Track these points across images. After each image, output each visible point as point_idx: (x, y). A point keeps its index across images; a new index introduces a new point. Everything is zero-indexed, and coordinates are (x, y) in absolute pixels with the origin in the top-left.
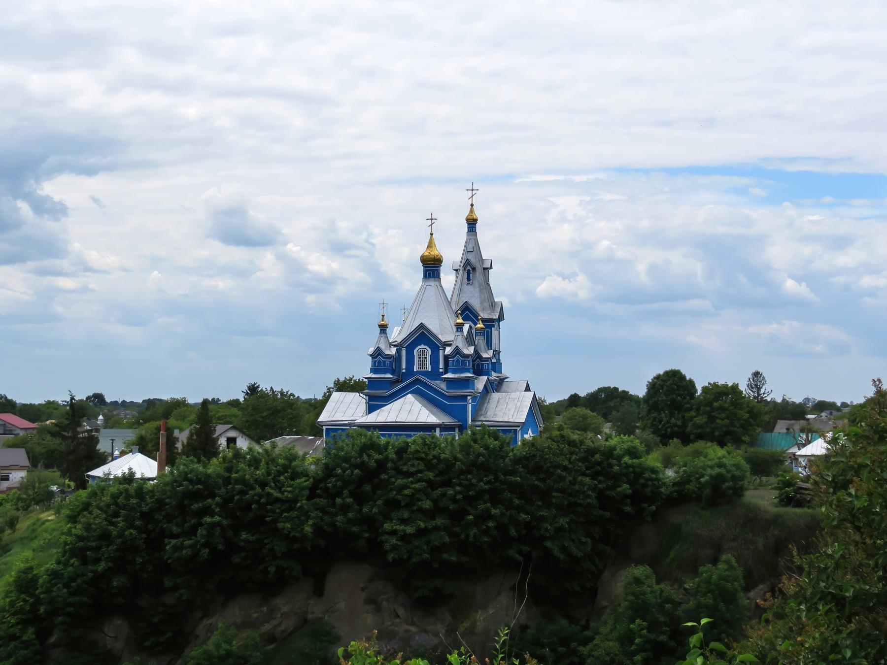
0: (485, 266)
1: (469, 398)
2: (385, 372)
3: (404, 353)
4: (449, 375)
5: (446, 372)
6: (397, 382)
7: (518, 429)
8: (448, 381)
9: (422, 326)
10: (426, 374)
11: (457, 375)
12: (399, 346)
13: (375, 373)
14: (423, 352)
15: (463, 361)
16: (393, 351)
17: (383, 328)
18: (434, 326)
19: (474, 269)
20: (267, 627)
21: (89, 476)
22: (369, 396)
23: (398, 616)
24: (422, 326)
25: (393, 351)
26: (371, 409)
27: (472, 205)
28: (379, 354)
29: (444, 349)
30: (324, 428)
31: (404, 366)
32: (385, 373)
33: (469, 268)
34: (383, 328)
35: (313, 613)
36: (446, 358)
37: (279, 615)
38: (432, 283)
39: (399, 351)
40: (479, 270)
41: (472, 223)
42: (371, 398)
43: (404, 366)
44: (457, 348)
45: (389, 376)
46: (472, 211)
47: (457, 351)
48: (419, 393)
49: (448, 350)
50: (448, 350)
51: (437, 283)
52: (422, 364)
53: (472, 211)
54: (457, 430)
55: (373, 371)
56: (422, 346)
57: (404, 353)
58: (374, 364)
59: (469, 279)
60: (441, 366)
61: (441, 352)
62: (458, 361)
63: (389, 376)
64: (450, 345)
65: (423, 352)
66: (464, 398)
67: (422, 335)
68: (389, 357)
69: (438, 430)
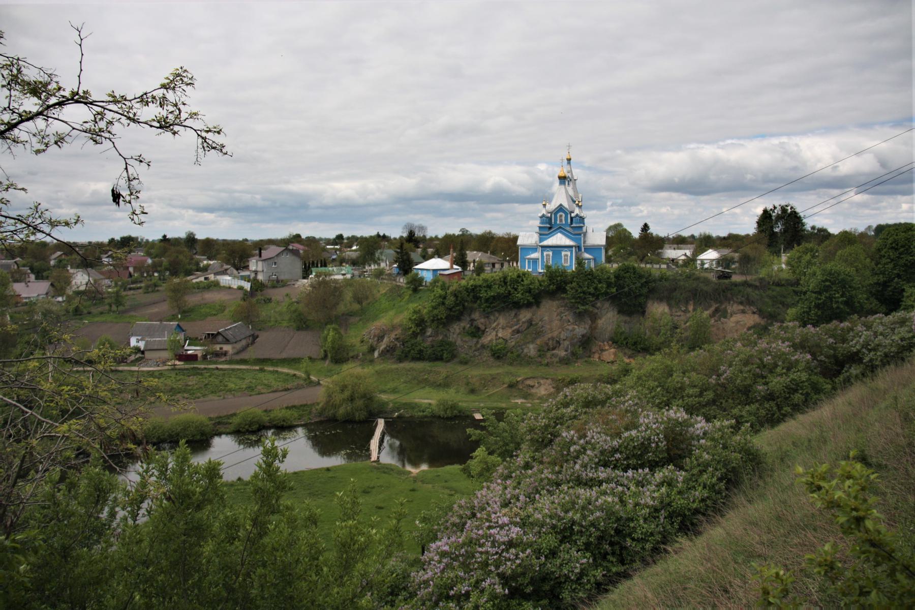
4: (574, 225)
6: (550, 228)
9: (561, 205)
12: (551, 213)
18: (566, 205)
20: (515, 327)
24: (561, 205)
36: (572, 218)
41: (569, 160)
42: (541, 234)
45: (549, 225)
48: (561, 232)
49: (573, 215)
50: (573, 215)
52: (561, 220)
55: (542, 223)
67: (561, 208)
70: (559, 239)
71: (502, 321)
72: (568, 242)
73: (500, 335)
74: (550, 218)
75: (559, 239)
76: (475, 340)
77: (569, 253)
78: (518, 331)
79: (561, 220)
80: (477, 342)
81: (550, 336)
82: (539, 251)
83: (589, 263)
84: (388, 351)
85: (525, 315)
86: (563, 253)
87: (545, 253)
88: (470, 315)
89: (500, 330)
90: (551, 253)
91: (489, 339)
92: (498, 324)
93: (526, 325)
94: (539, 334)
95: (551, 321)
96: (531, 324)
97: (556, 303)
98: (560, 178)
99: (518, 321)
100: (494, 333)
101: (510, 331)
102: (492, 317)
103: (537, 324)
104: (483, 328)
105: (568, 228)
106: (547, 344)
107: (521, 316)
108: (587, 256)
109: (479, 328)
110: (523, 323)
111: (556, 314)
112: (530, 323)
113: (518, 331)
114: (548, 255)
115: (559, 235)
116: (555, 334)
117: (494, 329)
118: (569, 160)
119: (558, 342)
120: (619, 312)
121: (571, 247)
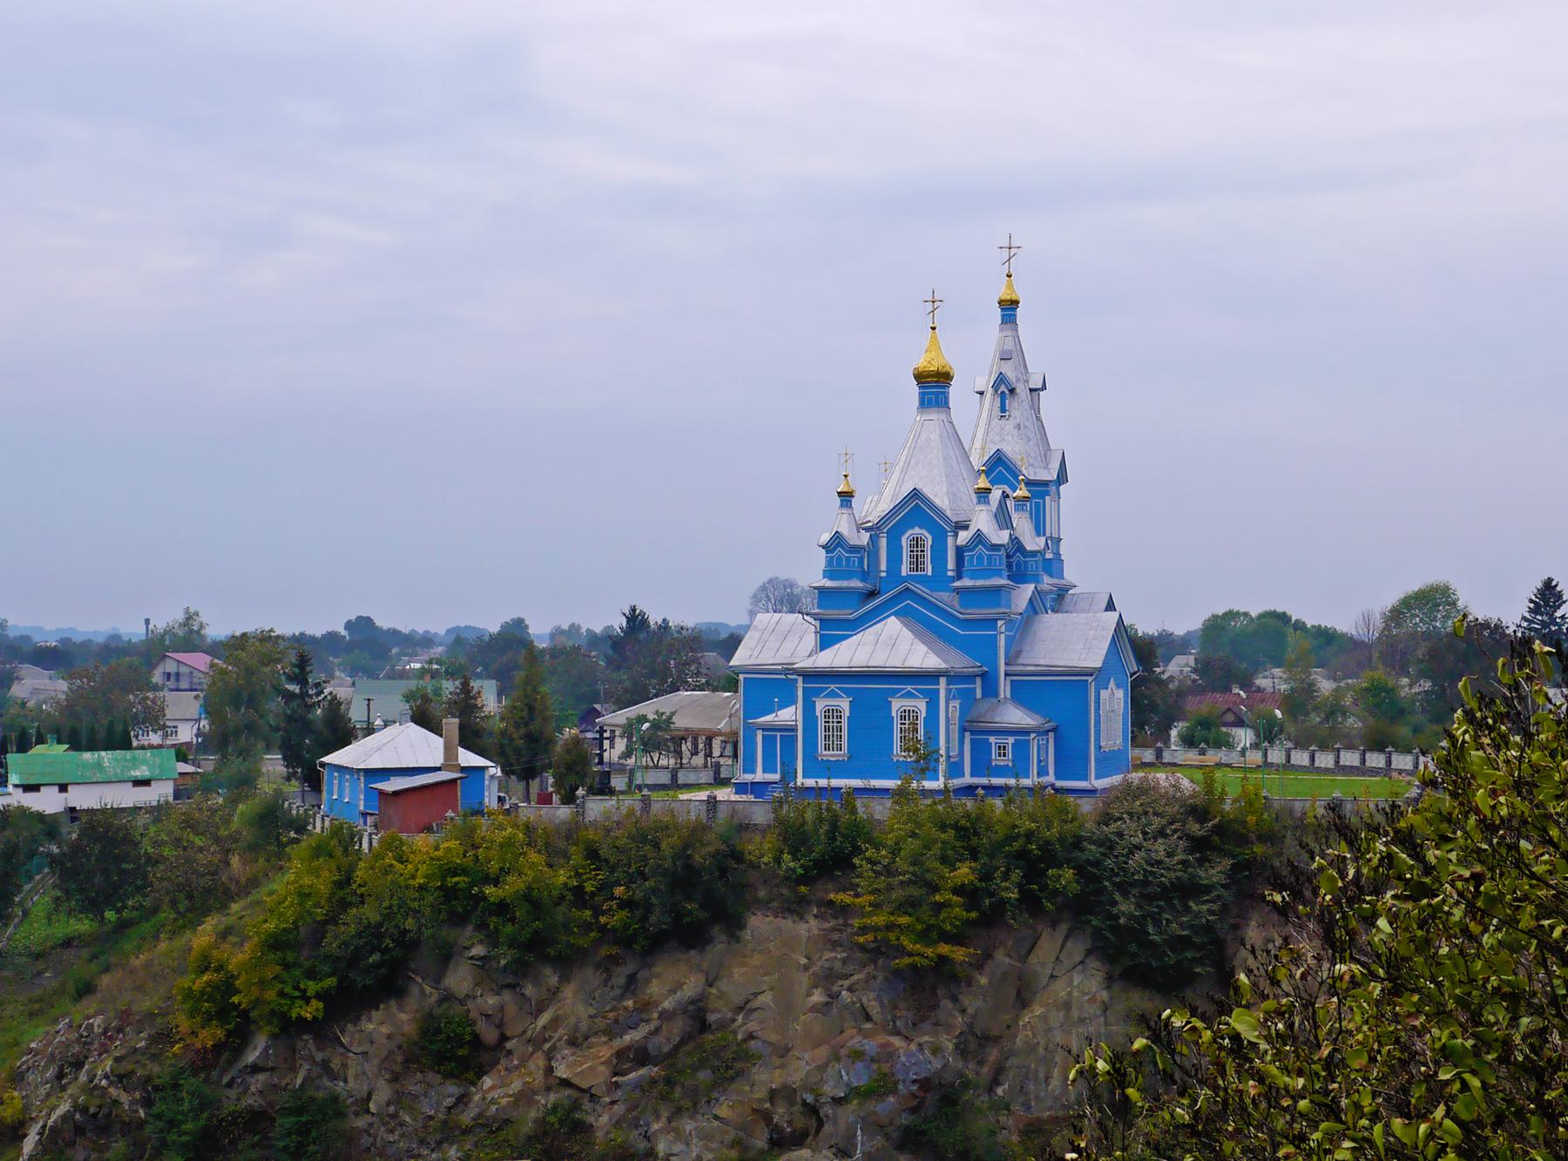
1: (1000, 623)
2: (848, 575)
3: (883, 542)
4: (966, 582)
5: (959, 577)
6: (872, 594)
7: (1090, 679)
8: (958, 590)
9: (915, 494)
10: (924, 580)
11: (980, 583)
13: (831, 579)
14: (917, 542)
15: (990, 557)
16: (864, 538)
17: (846, 497)
18: (939, 496)
19: (1012, 391)
21: (323, 765)
23: (868, 1018)
24: (915, 494)
25: (864, 538)
26: (825, 643)
27: (1009, 276)
28: (839, 544)
29: (956, 535)
30: (741, 677)
31: (883, 567)
32: (848, 579)
33: (1003, 388)
34: (846, 497)
35: (718, 1011)
36: (960, 551)
37: (656, 1015)
38: (934, 416)
39: (874, 540)
40: (1022, 391)
41: (1009, 307)
42: (825, 623)
43: (883, 567)
44: (979, 534)
45: (858, 584)
46: (1010, 286)
47: (979, 537)
49: (964, 537)
50: (964, 537)
51: (943, 416)
52: (917, 563)
53: (1010, 286)
54: (978, 681)
55: (830, 573)
56: (917, 530)
57: (883, 542)
58: (829, 562)
59: (1003, 409)
60: (951, 564)
61: (950, 540)
62: (980, 557)
63: (856, 583)
64: (966, 528)
65: (917, 542)
66: (991, 622)
67: (915, 508)
68: (856, 549)
69: (943, 681)
70: (890, 644)
71: (574, 1002)
72: (919, 655)
73: (562, 1071)
75: (890, 644)
76: (453, 1089)
77: (921, 706)
78: (641, 1056)
80: (463, 1100)
81: (776, 1079)
82: (811, 687)
83: (1022, 750)
84: (79, 1130)
85: (672, 983)
86: (897, 705)
87: (820, 705)
88: (438, 980)
89: (566, 1044)
90: (844, 705)
91: (516, 1086)
92: (555, 1022)
93: (677, 1028)
94: (731, 1065)
95: (787, 1009)
96: (704, 1027)
97: (809, 927)
98: (921, 377)
99: (645, 1007)
100: (538, 1062)
101: (606, 1052)
102: (529, 990)
103: (724, 1025)
104: (489, 1035)
105: (944, 598)
106: (767, 1117)
107: (655, 989)
108: (1016, 716)
109: (476, 1040)
110: (666, 1016)
111: (805, 980)
112: (697, 1016)
113: (641, 1056)
114: (828, 713)
115: (892, 625)
116: (799, 1070)
117: (537, 1042)
118: (1009, 307)
119: (812, 1110)
120: (1109, 980)
121: (930, 677)
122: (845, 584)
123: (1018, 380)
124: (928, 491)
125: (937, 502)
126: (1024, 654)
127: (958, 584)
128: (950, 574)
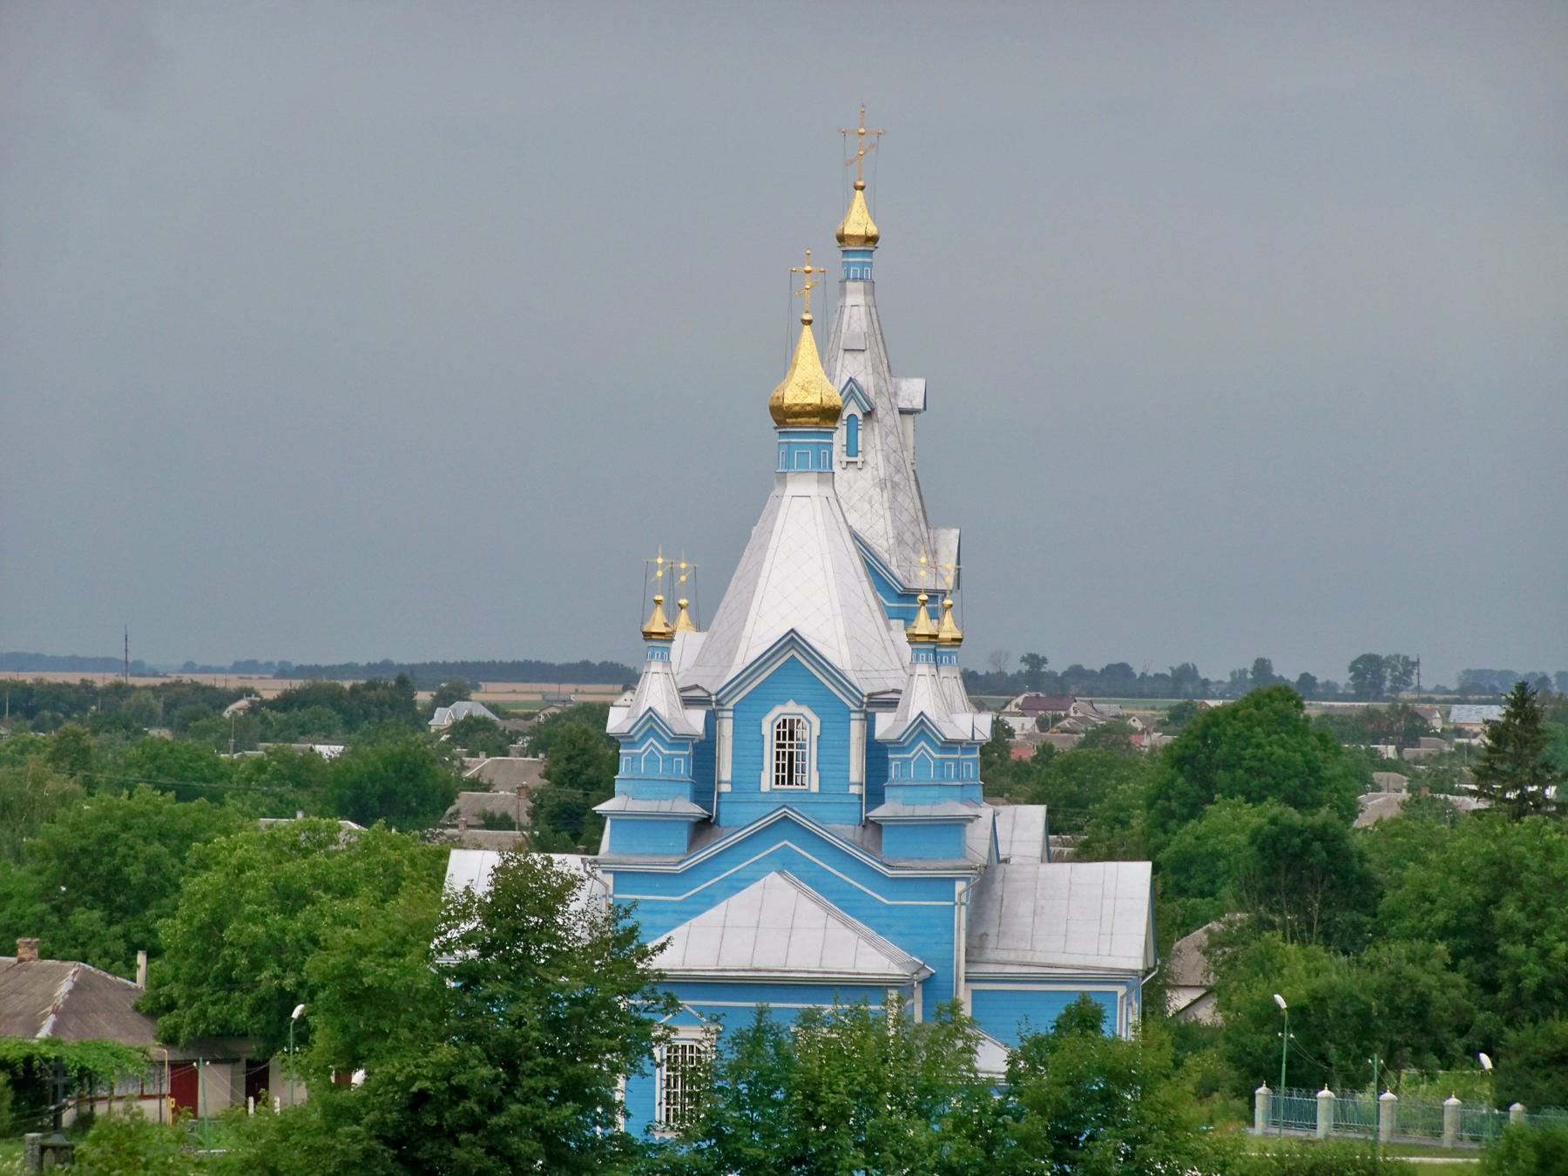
0: (904, 405)
1: (960, 886)
3: (726, 728)
6: (703, 827)
9: (792, 640)
10: (806, 798)
11: (923, 810)
14: (787, 731)
19: (869, 415)
22: (615, 873)
24: (792, 640)
25: (695, 720)
28: (651, 732)
36: (877, 753)
39: (711, 721)
47: (922, 728)
48: (785, 864)
49: (886, 725)
50: (886, 725)
51: (827, 491)
52: (788, 770)
56: (791, 709)
62: (923, 762)
64: (892, 705)
65: (787, 731)
68: (679, 741)
69: (893, 994)
74: (704, 752)
79: (788, 770)
122: (665, 807)
123: (879, 392)
124: (812, 634)
125: (838, 665)
126: (992, 942)
127: (878, 813)
128: (854, 789)
